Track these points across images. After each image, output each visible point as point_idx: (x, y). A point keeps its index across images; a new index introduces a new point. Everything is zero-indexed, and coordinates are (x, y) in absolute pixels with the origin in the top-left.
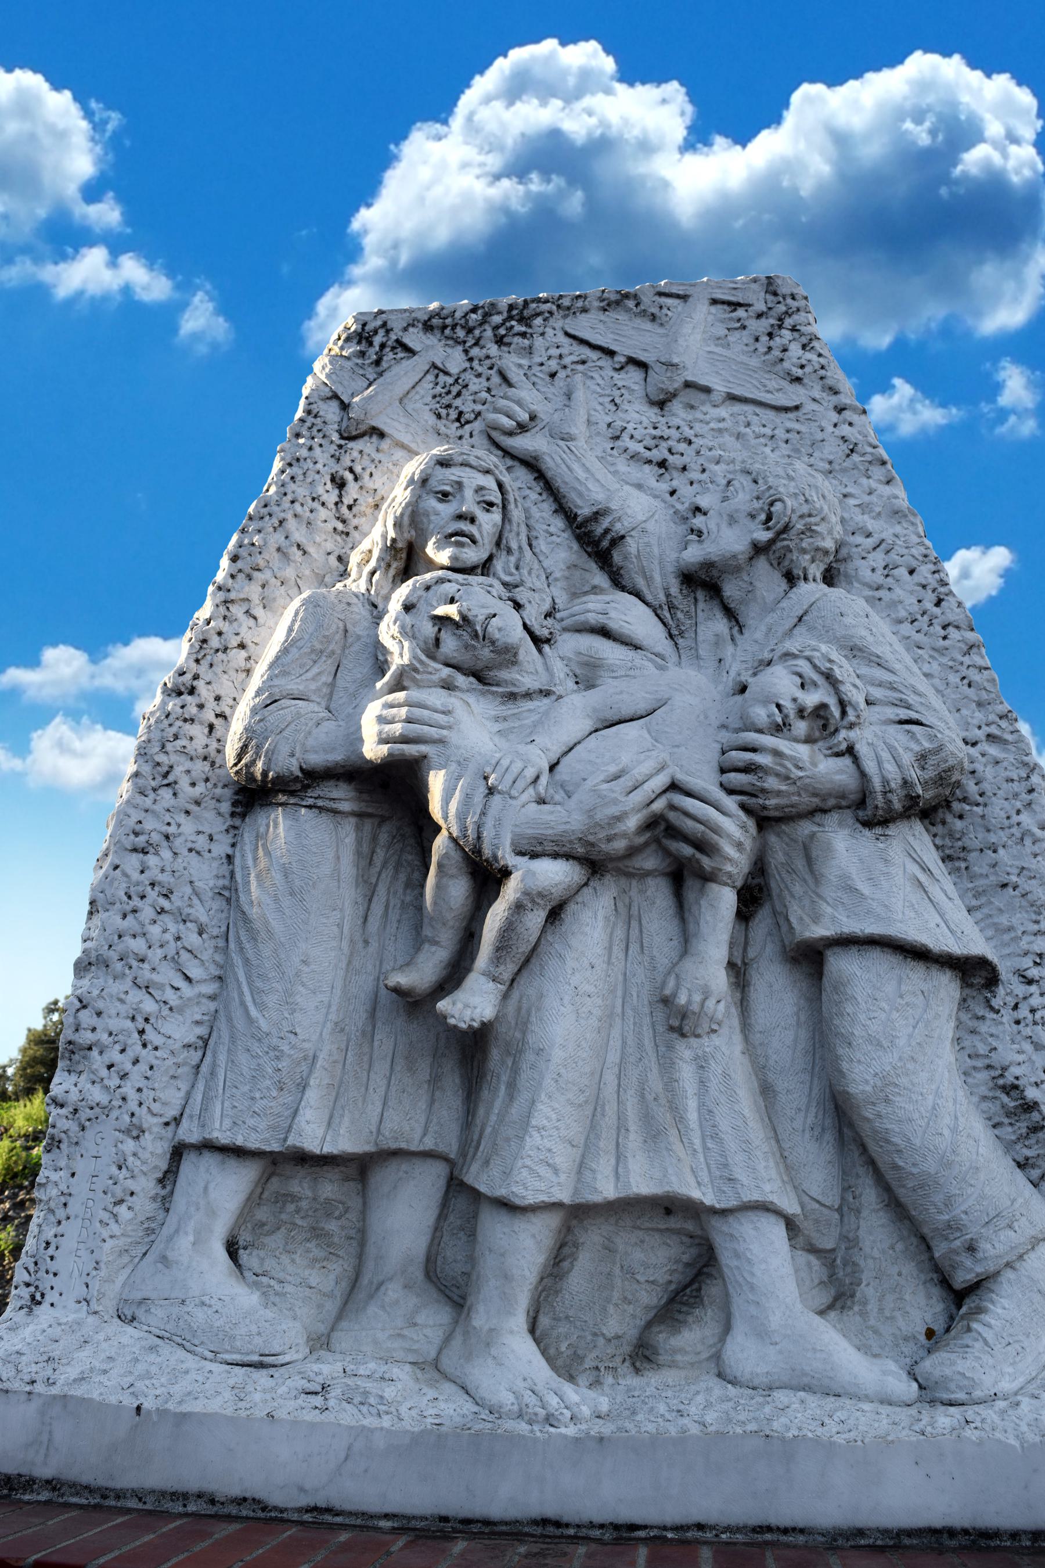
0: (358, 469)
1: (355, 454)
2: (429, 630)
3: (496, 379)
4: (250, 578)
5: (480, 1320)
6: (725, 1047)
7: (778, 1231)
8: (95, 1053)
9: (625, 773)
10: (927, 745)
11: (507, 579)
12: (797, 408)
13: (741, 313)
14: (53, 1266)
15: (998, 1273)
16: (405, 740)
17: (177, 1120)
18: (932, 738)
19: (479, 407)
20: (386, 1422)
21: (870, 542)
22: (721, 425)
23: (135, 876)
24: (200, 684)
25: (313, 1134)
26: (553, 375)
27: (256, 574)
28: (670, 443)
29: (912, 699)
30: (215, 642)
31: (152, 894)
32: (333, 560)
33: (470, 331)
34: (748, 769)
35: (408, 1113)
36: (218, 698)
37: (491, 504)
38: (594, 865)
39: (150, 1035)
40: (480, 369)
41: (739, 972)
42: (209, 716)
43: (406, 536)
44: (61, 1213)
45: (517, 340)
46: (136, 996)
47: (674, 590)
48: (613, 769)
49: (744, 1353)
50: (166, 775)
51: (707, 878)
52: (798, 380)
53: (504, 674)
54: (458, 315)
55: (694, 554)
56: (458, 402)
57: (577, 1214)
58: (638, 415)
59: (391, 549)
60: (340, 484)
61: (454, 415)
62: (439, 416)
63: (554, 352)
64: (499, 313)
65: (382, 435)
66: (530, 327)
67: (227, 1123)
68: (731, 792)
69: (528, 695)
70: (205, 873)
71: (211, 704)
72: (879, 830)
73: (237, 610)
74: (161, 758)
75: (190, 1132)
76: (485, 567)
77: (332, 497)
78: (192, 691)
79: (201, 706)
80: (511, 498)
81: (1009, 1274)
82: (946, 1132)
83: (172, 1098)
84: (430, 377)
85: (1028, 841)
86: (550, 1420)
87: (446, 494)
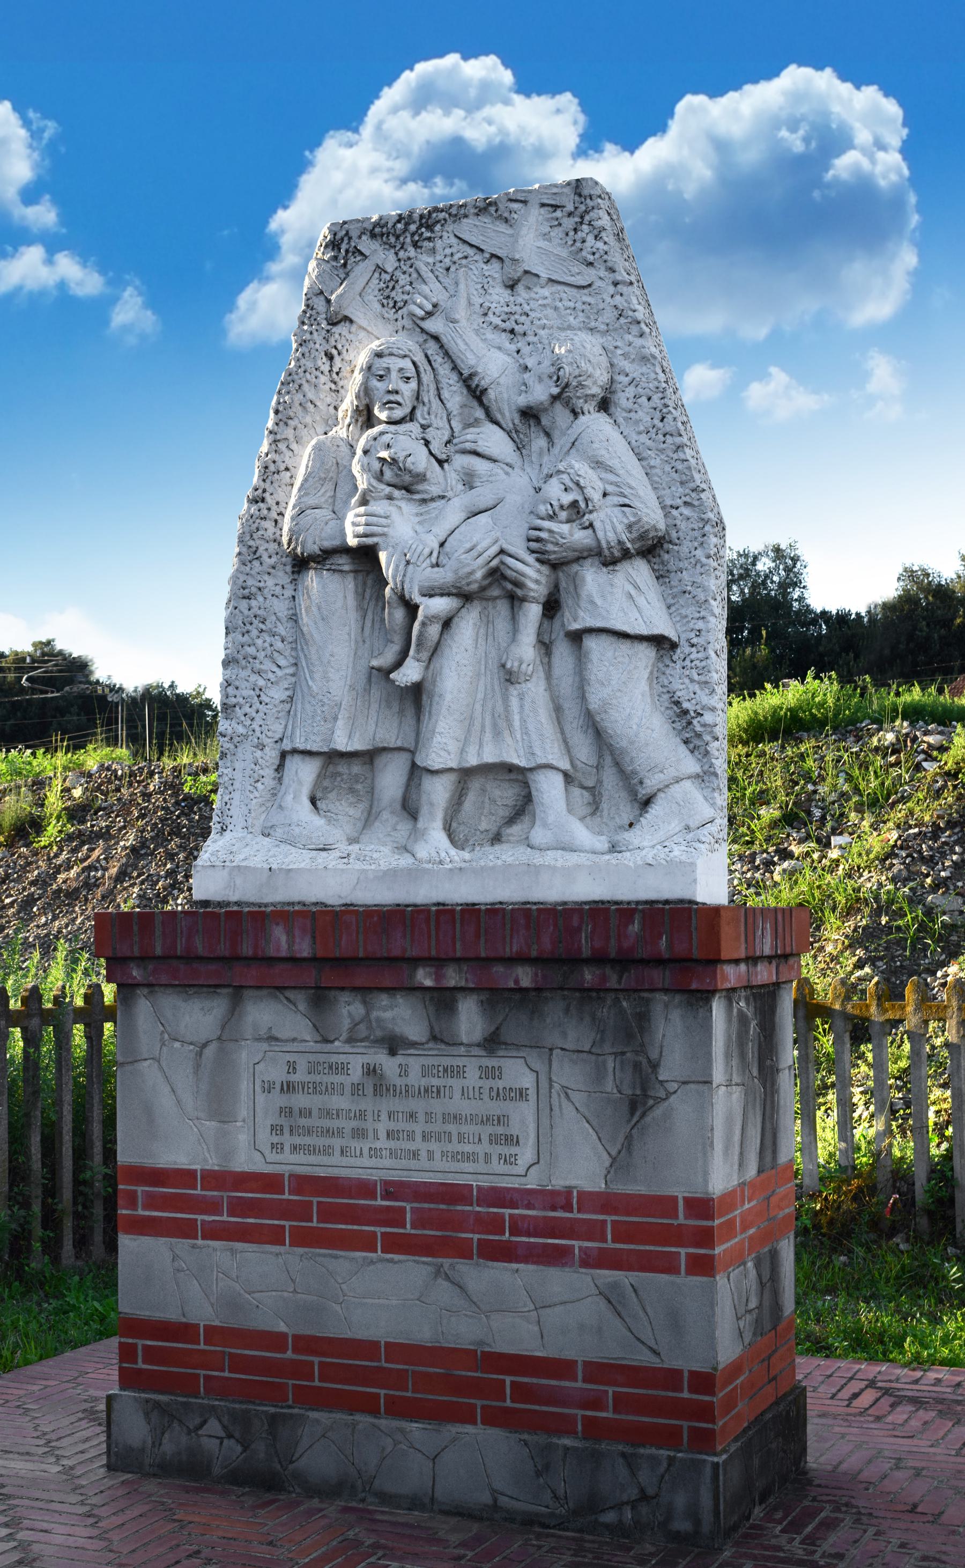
0: (339, 347)
1: (337, 336)
2: (377, 466)
3: (415, 275)
4: (286, 424)
5: (421, 824)
6: (536, 689)
7: (559, 779)
8: (237, 708)
9: (479, 543)
10: (632, 519)
11: (423, 422)
12: (590, 285)
13: (558, 213)
14: (230, 813)
15: (655, 794)
16: (365, 535)
17: (281, 740)
18: (635, 515)
19: (406, 297)
20: (373, 867)
21: (626, 380)
22: (545, 302)
23: (246, 612)
24: (267, 495)
25: (342, 743)
26: (448, 269)
27: (290, 422)
28: (517, 317)
29: (627, 491)
30: (272, 468)
31: (256, 622)
32: (331, 408)
33: (398, 237)
34: (538, 540)
35: (383, 729)
36: (278, 503)
37: (408, 378)
38: (466, 597)
39: (263, 698)
40: (405, 268)
41: (545, 646)
42: (274, 515)
43: (364, 402)
44: (231, 788)
45: (426, 244)
46: (254, 678)
47: (517, 421)
48: (468, 546)
49: (539, 835)
50: (255, 553)
51: (523, 600)
52: (591, 264)
53: (420, 487)
54: (390, 225)
55: (522, 401)
56: (393, 294)
57: (466, 774)
58: (499, 296)
59: (357, 411)
60: (331, 358)
61: (391, 305)
62: (383, 306)
63: (448, 251)
64: (414, 222)
65: (351, 321)
66: (432, 231)
67: (303, 739)
68: (533, 552)
69: (432, 499)
70: (281, 607)
71: (274, 507)
72: (611, 568)
73: (282, 446)
74: (251, 543)
75: (287, 745)
76: (411, 417)
77: (326, 368)
78: (263, 500)
79: (269, 509)
80: (421, 370)
81: (661, 795)
82: (635, 727)
83: (278, 729)
84: (376, 275)
85: (698, 566)
86: (441, 862)
87: (381, 376)
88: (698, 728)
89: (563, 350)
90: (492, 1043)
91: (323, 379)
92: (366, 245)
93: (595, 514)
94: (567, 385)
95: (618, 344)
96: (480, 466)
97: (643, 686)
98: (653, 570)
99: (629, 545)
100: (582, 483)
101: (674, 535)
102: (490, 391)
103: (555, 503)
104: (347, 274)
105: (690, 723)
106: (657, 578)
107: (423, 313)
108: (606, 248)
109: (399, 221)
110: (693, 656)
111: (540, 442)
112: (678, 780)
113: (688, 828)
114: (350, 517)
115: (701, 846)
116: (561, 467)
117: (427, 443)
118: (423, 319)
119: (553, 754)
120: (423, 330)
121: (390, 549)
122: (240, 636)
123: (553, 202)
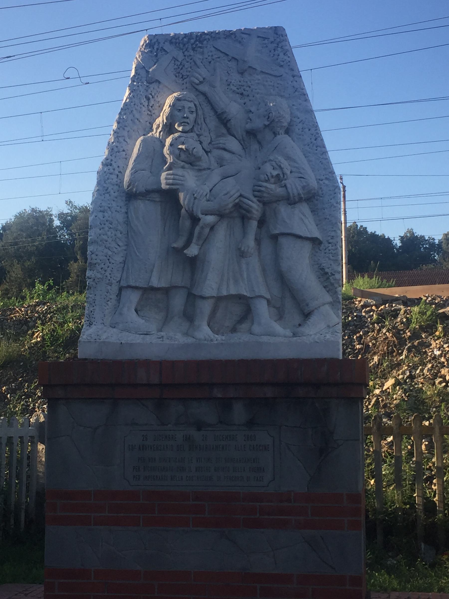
0: (153, 94)
1: (152, 89)
2: (177, 152)
3: (193, 63)
4: (124, 129)
5: (196, 323)
7: (265, 302)
8: (97, 265)
10: (305, 184)
11: (198, 133)
12: (281, 76)
13: (266, 41)
14: (94, 316)
15: (313, 311)
16: (172, 184)
17: (120, 281)
18: (306, 182)
19: (188, 74)
20: (176, 342)
21: (298, 121)
22: (259, 81)
23: (102, 218)
24: (113, 163)
25: (155, 283)
26: (210, 62)
27: (125, 128)
28: (244, 87)
29: (302, 171)
30: (116, 149)
31: (107, 223)
32: (148, 123)
33: (184, 45)
34: (259, 191)
36: (118, 167)
37: (193, 112)
38: (221, 216)
39: (111, 260)
40: (188, 60)
41: (258, 241)
42: (117, 172)
43: (170, 122)
44: (94, 304)
45: (199, 49)
46: (106, 251)
47: (244, 136)
48: (225, 192)
49: (256, 329)
50: (107, 190)
51: (250, 219)
52: (282, 66)
53: (198, 163)
54: (180, 39)
55: (249, 126)
56: (181, 72)
57: (219, 299)
58: (235, 77)
60: (148, 99)
61: (181, 76)
62: (176, 77)
63: (210, 54)
64: (193, 39)
65: (159, 82)
66: (202, 44)
67: (134, 281)
68: (255, 196)
69: (204, 169)
70: (121, 218)
71: (117, 169)
72: (293, 206)
73: (121, 139)
74: (105, 185)
75: (123, 283)
76: (192, 130)
77: (146, 104)
78: (111, 165)
79: (114, 169)
80: (198, 109)
81: (316, 310)
82: (304, 279)
83: (118, 275)
84: (173, 62)
85: (332, 207)
86: (212, 340)
87: (180, 110)
88: (332, 281)
89: (271, 105)
90: (251, 423)
91: (144, 109)
92: (167, 47)
93: (287, 180)
94: (273, 120)
95: (294, 103)
96: (226, 155)
97: (307, 261)
98: (310, 208)
99: (302, 196)
100: (282, 166)
101: (320, 192)
102: (231, 120)
103: (269, 174)
104: (158, 60)
105: (328, 278)
106: (312, 212)
107: (199, 82)
108: (289, 59)
109: (185, 37)
110: (330, 248)
111: (255, 146)
112: (324, 304)
113: (328, 326)
114: (164, 175)
115: (338, 334)
116: (271, 158)
117: (201, 143)
118: (197, 85)
119: (263, 291)
120: (196, 89)
121: (186, 191)
122: (99, 230)
123: (264, 36)
